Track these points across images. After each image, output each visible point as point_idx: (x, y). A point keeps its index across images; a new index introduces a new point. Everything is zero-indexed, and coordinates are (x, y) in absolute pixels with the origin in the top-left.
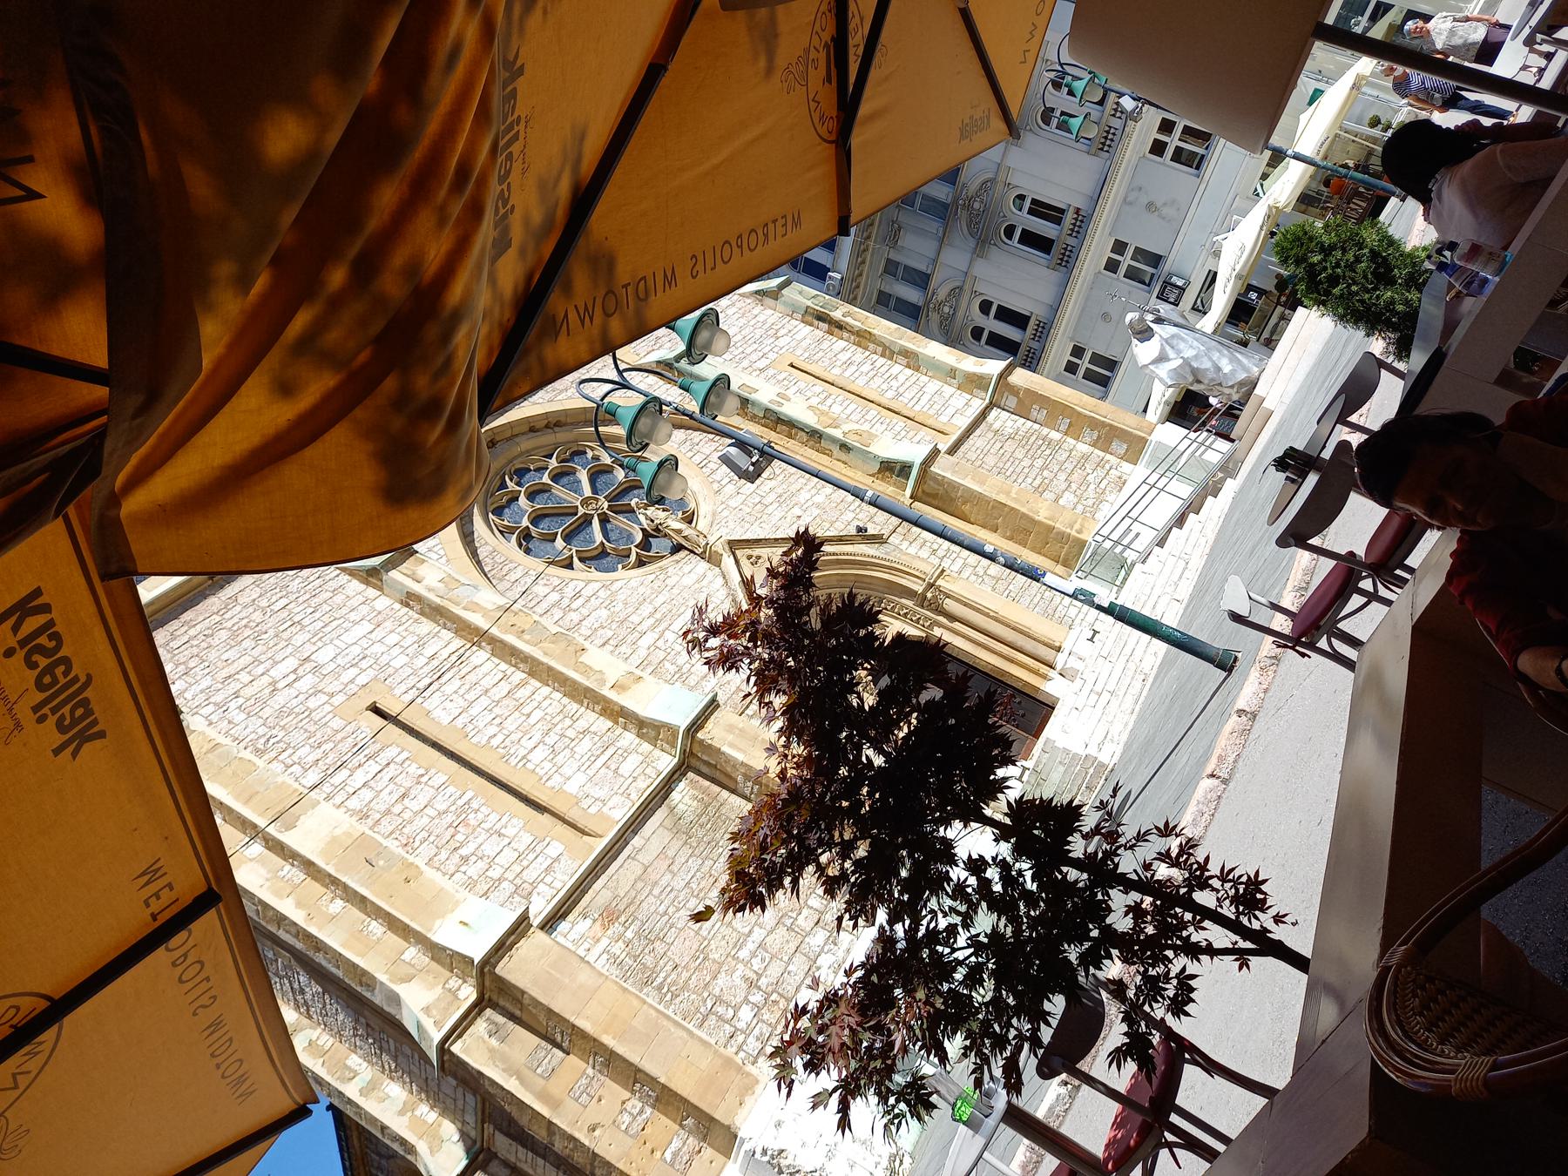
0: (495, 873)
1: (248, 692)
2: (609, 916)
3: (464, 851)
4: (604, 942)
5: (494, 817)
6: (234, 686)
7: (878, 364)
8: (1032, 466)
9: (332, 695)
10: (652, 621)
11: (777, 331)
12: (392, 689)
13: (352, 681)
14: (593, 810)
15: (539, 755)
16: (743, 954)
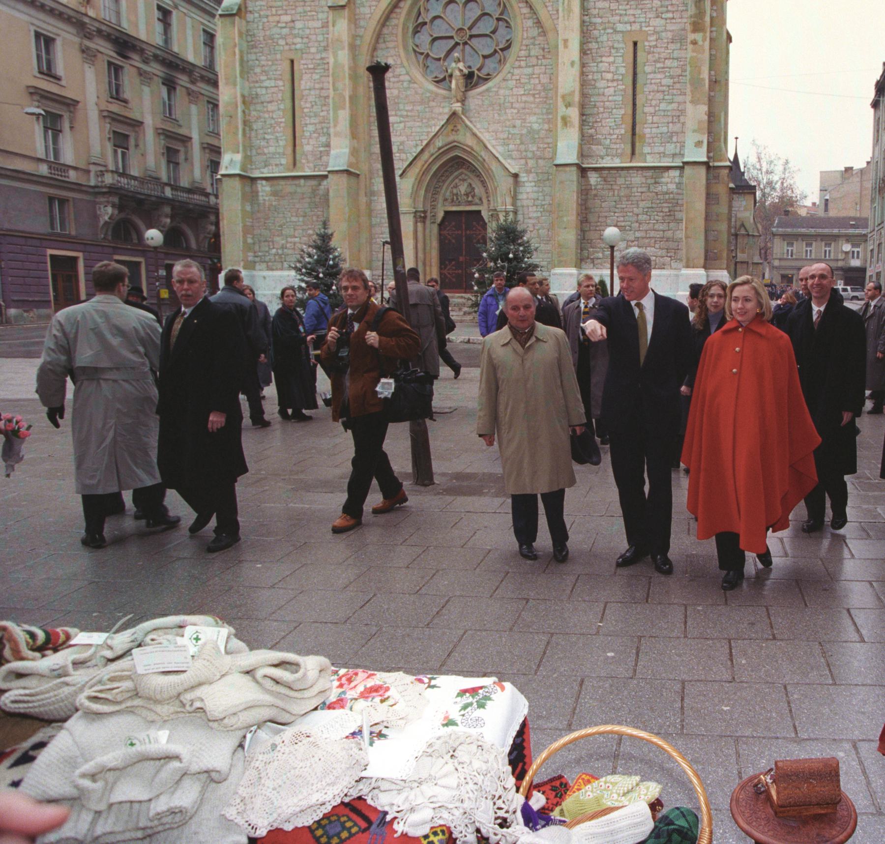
0: (266, 151)
1: (271, 19)
2: (275, 194)
3: (267, 136)
4: (267, 198)
5: (281, 134)
6: (269, 13)
7: (678, 86)
8: (638, 215)
9: (287, 44)
10: (405, 113)
11: (667, 12)
12: (302, 59)
13: (295, 44)
14: (304, 161)
15: (311, 128)
16: (289, 240)
